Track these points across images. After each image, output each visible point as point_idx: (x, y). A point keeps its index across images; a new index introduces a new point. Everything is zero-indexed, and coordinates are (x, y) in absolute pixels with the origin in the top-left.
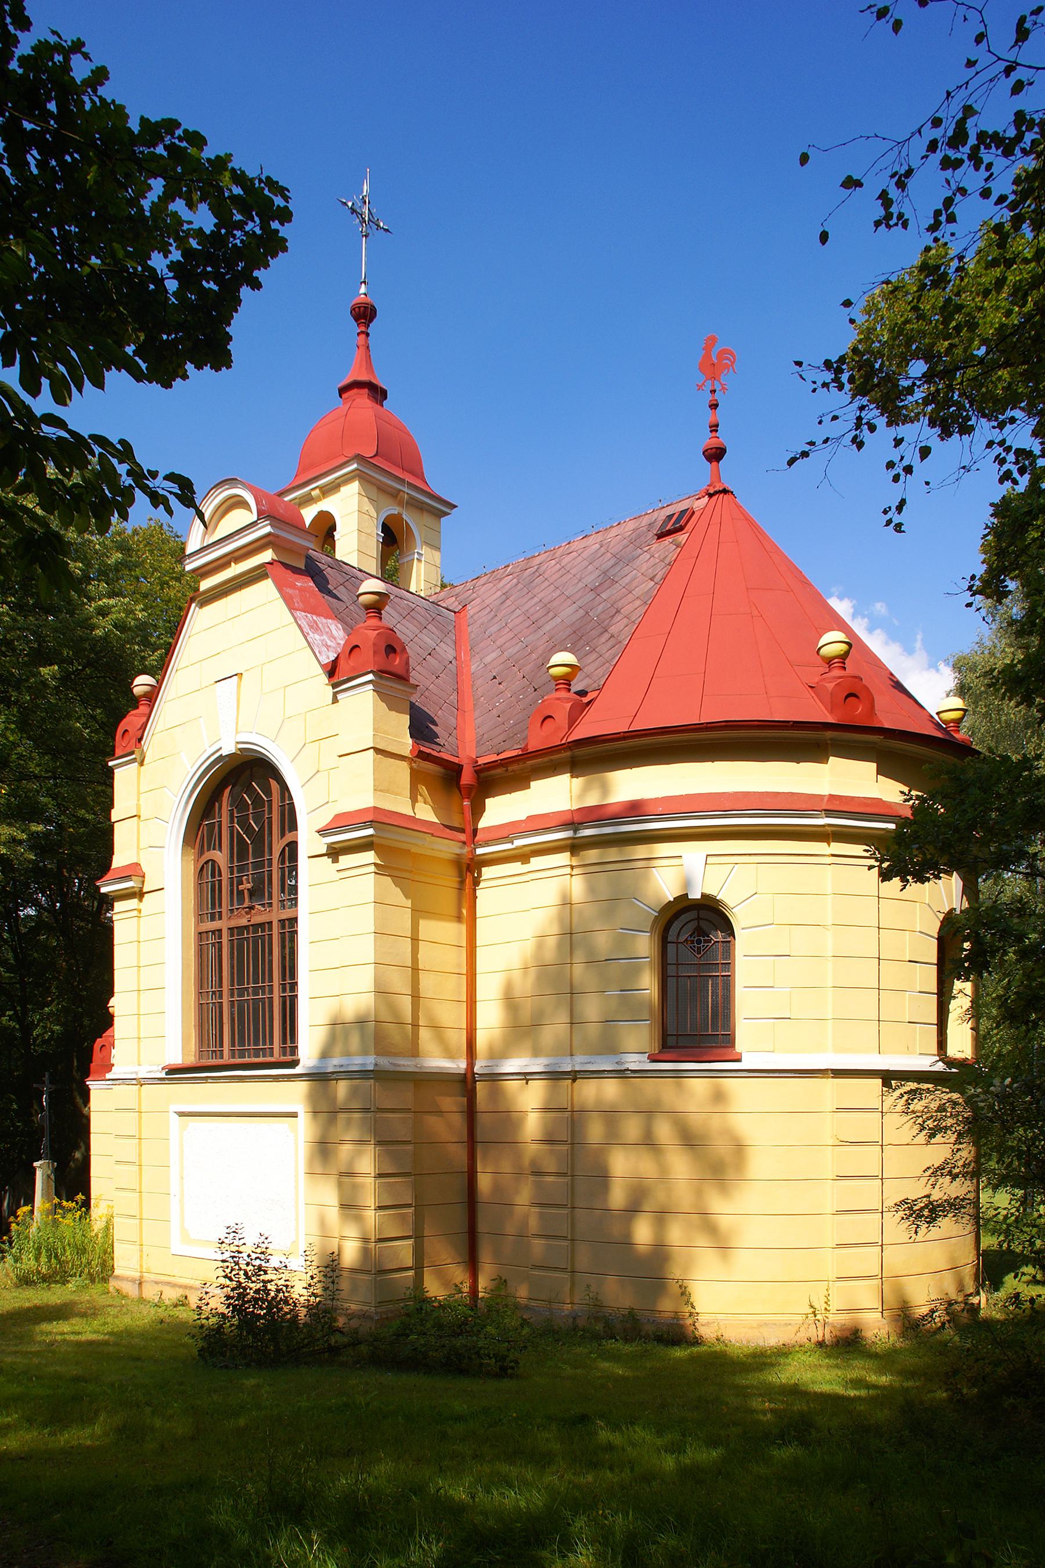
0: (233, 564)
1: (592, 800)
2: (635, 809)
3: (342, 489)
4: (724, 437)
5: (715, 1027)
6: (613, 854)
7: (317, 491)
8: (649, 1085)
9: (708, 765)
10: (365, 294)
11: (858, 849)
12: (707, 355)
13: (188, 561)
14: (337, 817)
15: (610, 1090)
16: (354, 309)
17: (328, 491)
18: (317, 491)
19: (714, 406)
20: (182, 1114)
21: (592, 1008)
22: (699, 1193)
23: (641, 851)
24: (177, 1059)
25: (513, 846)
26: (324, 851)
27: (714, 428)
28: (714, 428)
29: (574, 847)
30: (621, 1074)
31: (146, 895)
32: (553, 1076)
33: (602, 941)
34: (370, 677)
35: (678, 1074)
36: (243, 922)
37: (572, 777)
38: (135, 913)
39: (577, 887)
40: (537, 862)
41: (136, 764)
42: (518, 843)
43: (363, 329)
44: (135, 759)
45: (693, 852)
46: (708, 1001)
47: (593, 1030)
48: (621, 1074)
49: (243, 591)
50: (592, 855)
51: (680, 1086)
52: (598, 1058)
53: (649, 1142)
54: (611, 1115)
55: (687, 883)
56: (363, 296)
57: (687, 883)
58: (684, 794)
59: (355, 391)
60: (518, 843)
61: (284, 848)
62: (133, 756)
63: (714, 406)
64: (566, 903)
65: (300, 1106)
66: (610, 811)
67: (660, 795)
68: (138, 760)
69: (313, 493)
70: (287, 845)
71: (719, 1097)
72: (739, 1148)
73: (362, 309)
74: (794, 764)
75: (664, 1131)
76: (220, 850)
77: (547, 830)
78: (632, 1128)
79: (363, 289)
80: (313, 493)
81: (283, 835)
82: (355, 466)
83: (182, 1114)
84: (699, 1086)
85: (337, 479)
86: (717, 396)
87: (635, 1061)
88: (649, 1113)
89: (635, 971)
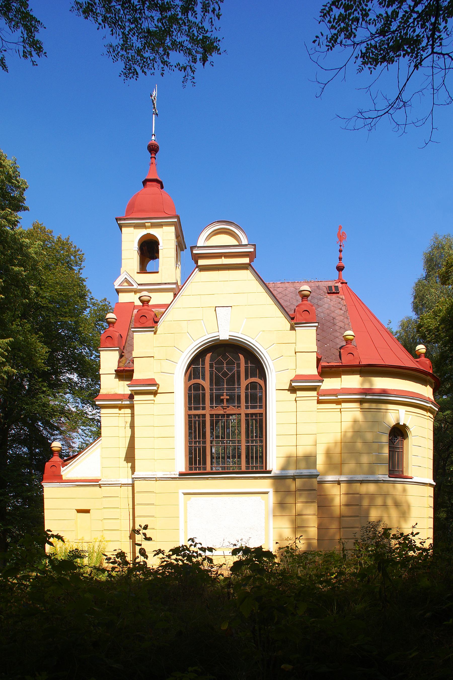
0: (223, 258)
1: (367, 386)
2: (384, 392)
3: (164, 228)
4: (343, 263)
5: (398, 468)
6: (374, 406)
7: (150, 224)
8: (385, 486)
9: (404, 381)
10: (155, 140)
11: (429, 414)
12: (339, 232)
13: (196, 249)
14: (297, 376)
15: (372, 488)
16: (150, 146)
17: (160, 225)
18: (150, 224)
19: (341, 251)
20: (185, 494)
21: (365, 459)
22: (399, 522)
23: (383, 406)
24: (183, 470)
25: (337, 398)
26: (288, 388)
27: (340, 259)
28: (340, 259)
29: (361, 402)
30: (376, 482)
31: (158, 394)
32: (349, 482)
33: (369, 436)
34: (317, 324)
35: (394, 482)
36: (222, 412)
37: (360, 377)
38: (153, 402)
39: (358, 415)
40: (344, 405)
41: (153, 333)
42: (339, 397)
43: (153, 156)
44: (154, 330)
45: (402, 409)
46: (395, 460)
47: (365, 467)
48: (376, 482)
49: (230, 271)
50: (366, 405)
51: (394, 487)
52: (368, 476)
53: (385, 505)
54: (372, 497)
55: (398, 420)
56: (153, 141)
57: (398, 420)
58: (393, 389)
59: (155, 183)
60: (339, 397)
61: (248, 384)
62: (153, 329)
63: (341, 251)
64: (355, 421)
65: (271, 490)
66: (373, 391)
67: (390, 389)
68: (154, 331)
69: (146, 224)
70: (250, 383)
71: (404, 490)
72: (409, 506)
73: (156, 147)
74: (421, 385)
75: (390, 502)
76: (204, 379)
77: (350, 394)
78: (379, 501)
79: (153, 138)
80: (146, 224)
81: (246, 378)
82: (176, 220)
83: (185, 494)
84: (399, 486)
85: (162, 222)
86: (342, 247)
87: (381, 477)
88: (385, 495)
89: (381, 447)
